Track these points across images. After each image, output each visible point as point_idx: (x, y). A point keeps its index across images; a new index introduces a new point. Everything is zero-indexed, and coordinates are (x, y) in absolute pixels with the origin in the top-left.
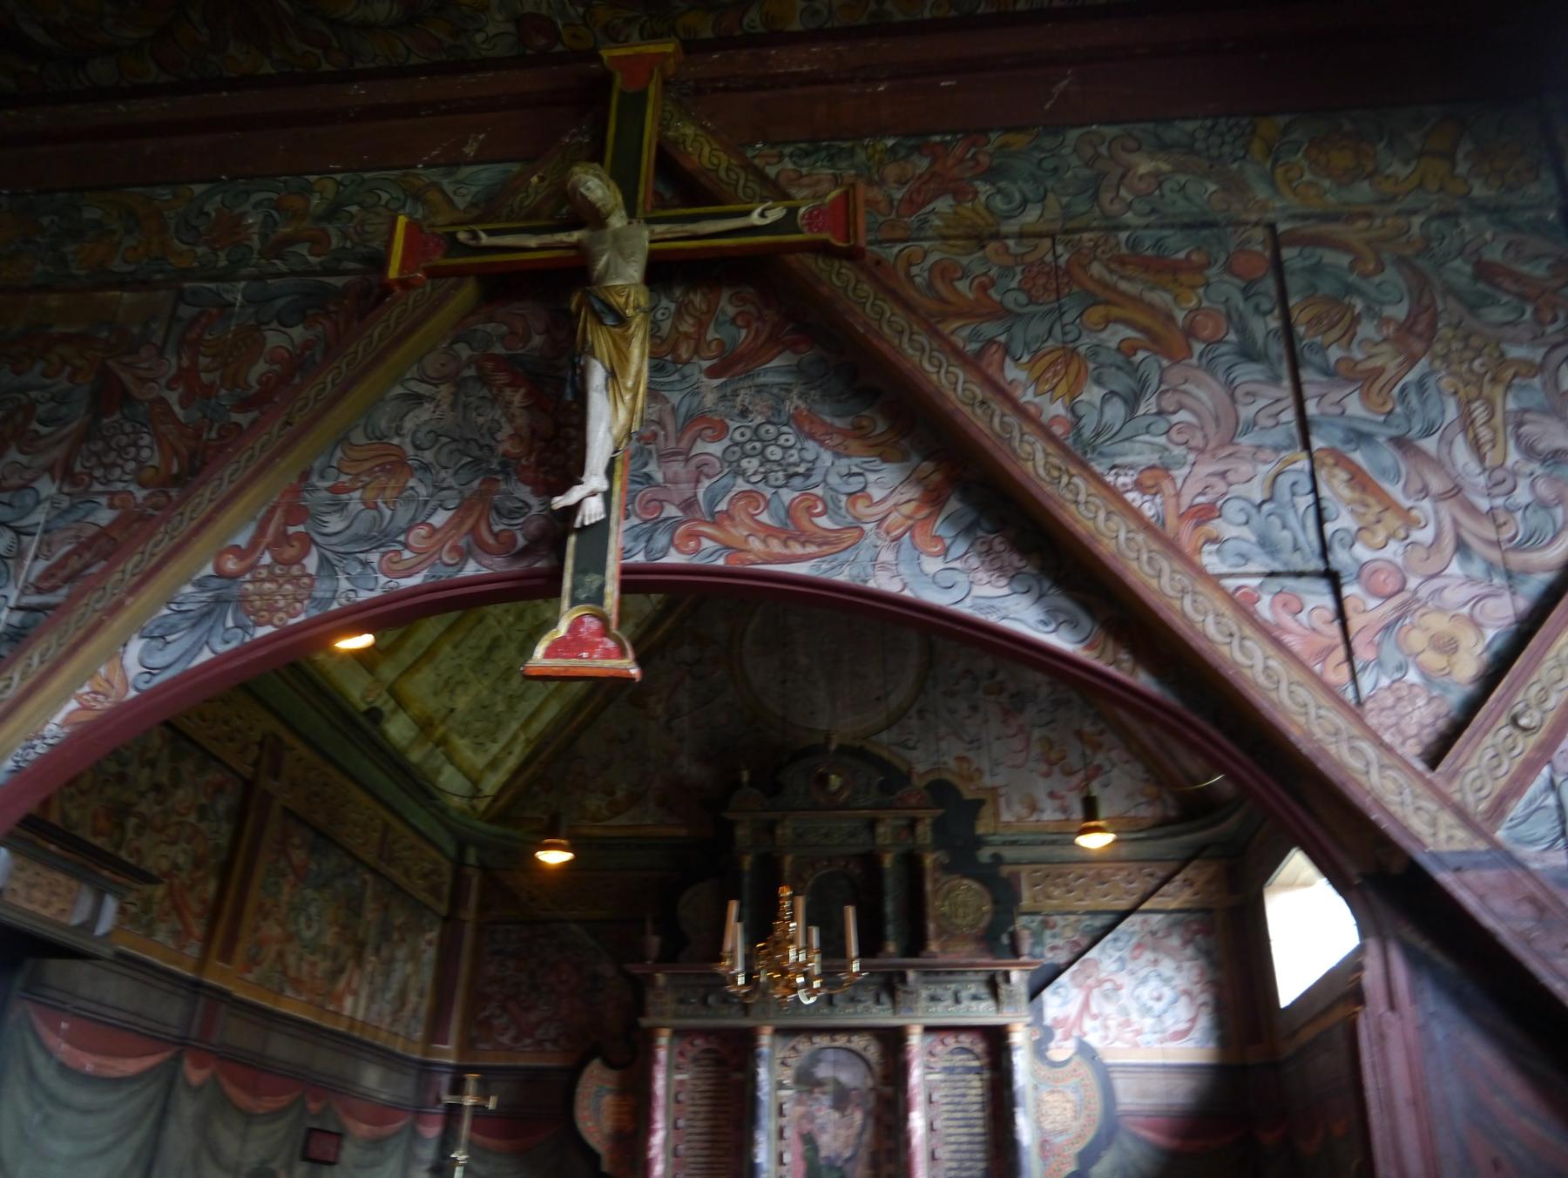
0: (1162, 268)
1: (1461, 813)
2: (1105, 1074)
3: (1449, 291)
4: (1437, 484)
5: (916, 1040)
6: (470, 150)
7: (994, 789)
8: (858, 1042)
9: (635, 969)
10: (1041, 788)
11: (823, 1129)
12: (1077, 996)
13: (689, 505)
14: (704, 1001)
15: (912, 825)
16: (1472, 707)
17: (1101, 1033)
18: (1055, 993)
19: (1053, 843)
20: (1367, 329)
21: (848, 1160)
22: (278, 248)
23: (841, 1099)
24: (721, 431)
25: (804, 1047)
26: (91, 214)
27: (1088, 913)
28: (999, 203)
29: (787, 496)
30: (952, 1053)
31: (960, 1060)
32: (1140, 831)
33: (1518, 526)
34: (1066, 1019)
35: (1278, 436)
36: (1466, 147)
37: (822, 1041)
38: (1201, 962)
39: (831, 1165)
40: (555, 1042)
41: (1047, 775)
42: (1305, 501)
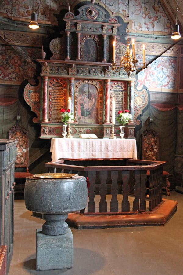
5: (109, 83)
7: (131, 20)
8: (95, 83)
9: (39, 60)
10: (143, 21)
11: (85, 103)
12: (145, 75)
14: (58, 70)
15: (112, 28)
17: (149, 84)
18: (140, 74)
19: (144, 36)
21: (90, 110)
23: (90, 96)
25: (81, 83)
27: (149, 55)
30: (116, 87)
31: (118, 88)
32: (165, 36)
34: (141, 80)
37: (86, 82)
38: (173, 69)
40: (15, 79)
41: (145, 18)
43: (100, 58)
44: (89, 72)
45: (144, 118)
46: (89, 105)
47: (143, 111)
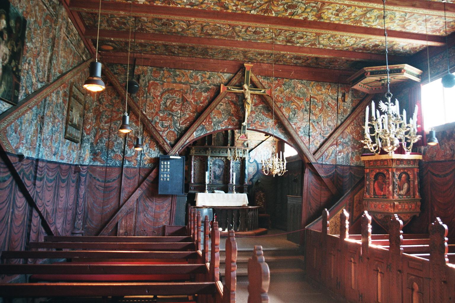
0: (299, 99)
1: (315, 159)
2: (258, 164)
3: (325, 105)
4: (320, 127)
6: (225, 71)
8: (223, 159)
13: (252, 122)
14: (200, 152)
16: (318, 149)
20: (317, 109)
22: (203, 82)
23: (219, 167)
24: (255, 113)
25: (214, 159)
26: (178, 73)
28: (284, 88)
29: (261, 122)
33: (325, 132)
35: (307, 120)
36: (330, 88)
39: (218, 176)
42: (308, 128)
43: (226, 144)
44: (219, 152)
45: (255, 180)
46: (218, 172)
47: (254, 176)
